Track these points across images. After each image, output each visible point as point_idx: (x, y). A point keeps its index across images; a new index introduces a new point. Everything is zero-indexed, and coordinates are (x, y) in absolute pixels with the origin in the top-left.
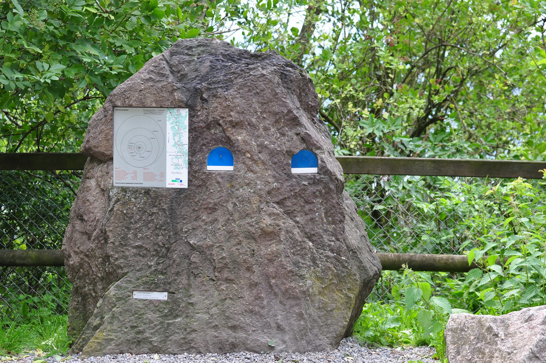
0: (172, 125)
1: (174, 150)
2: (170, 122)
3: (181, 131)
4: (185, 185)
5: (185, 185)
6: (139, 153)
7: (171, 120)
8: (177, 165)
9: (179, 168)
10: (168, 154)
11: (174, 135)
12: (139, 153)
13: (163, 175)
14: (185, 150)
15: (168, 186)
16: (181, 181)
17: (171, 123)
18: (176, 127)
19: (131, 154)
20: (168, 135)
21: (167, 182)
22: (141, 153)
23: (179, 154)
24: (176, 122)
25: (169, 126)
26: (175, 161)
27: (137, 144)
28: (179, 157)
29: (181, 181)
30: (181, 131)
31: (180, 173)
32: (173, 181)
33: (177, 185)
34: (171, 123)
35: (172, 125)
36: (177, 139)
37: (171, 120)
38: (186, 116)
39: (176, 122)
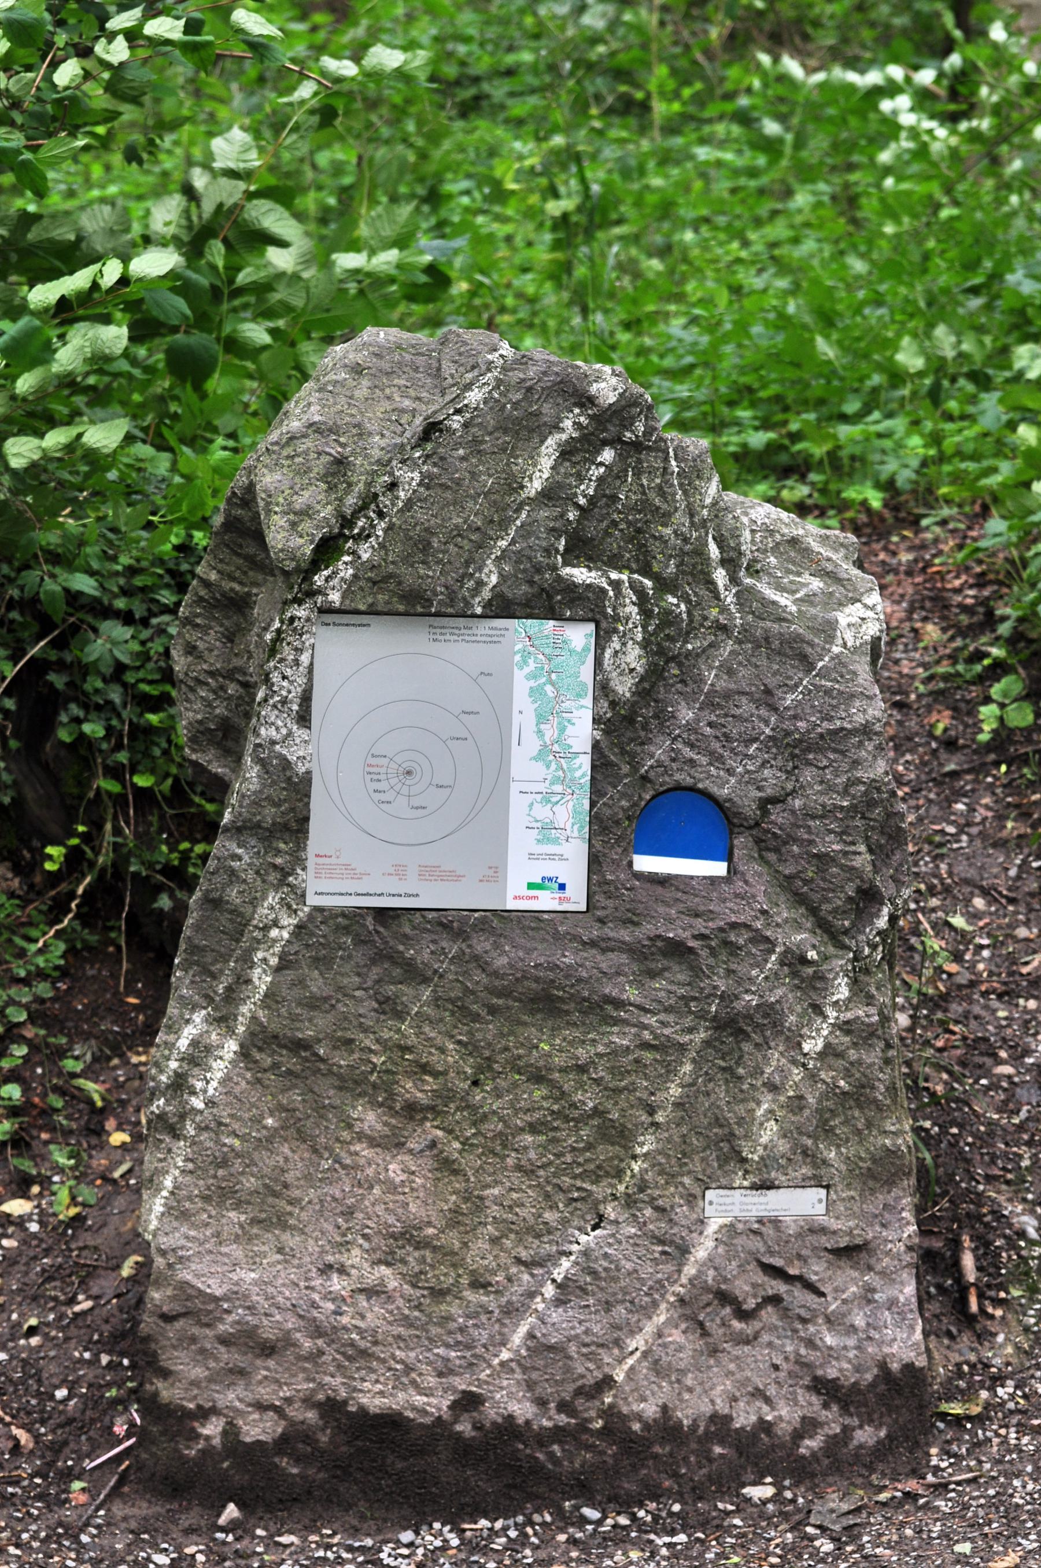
0: (532, 683)
1: (539, 770)
2: (527, 670)
3: (567, 705)
5: (577, 899)
7: (532, 665)
8: (547, 830)
9: (556, 841)
10: (514, 788)
11: (541, 719)
14: (578, 774)
16: (562, 887)
17: (528, 677)
18: (549, 688)
20: (516, 718)
21: (510, 895)
22: (414, 790)
23: (558, 788)
24: (550, 672)
25: (521, 685)
26: (543, 812)
27: (398, 759)
28: (554, 799)
29: (562, 887)
30: (567, 705)
31: (562, 858)
32: (531, 886)
33: (546, 901)
34: (530, 677)
35: (532, 683)
36: (550, 732)
37: (532, 665)
38: (586, 649)
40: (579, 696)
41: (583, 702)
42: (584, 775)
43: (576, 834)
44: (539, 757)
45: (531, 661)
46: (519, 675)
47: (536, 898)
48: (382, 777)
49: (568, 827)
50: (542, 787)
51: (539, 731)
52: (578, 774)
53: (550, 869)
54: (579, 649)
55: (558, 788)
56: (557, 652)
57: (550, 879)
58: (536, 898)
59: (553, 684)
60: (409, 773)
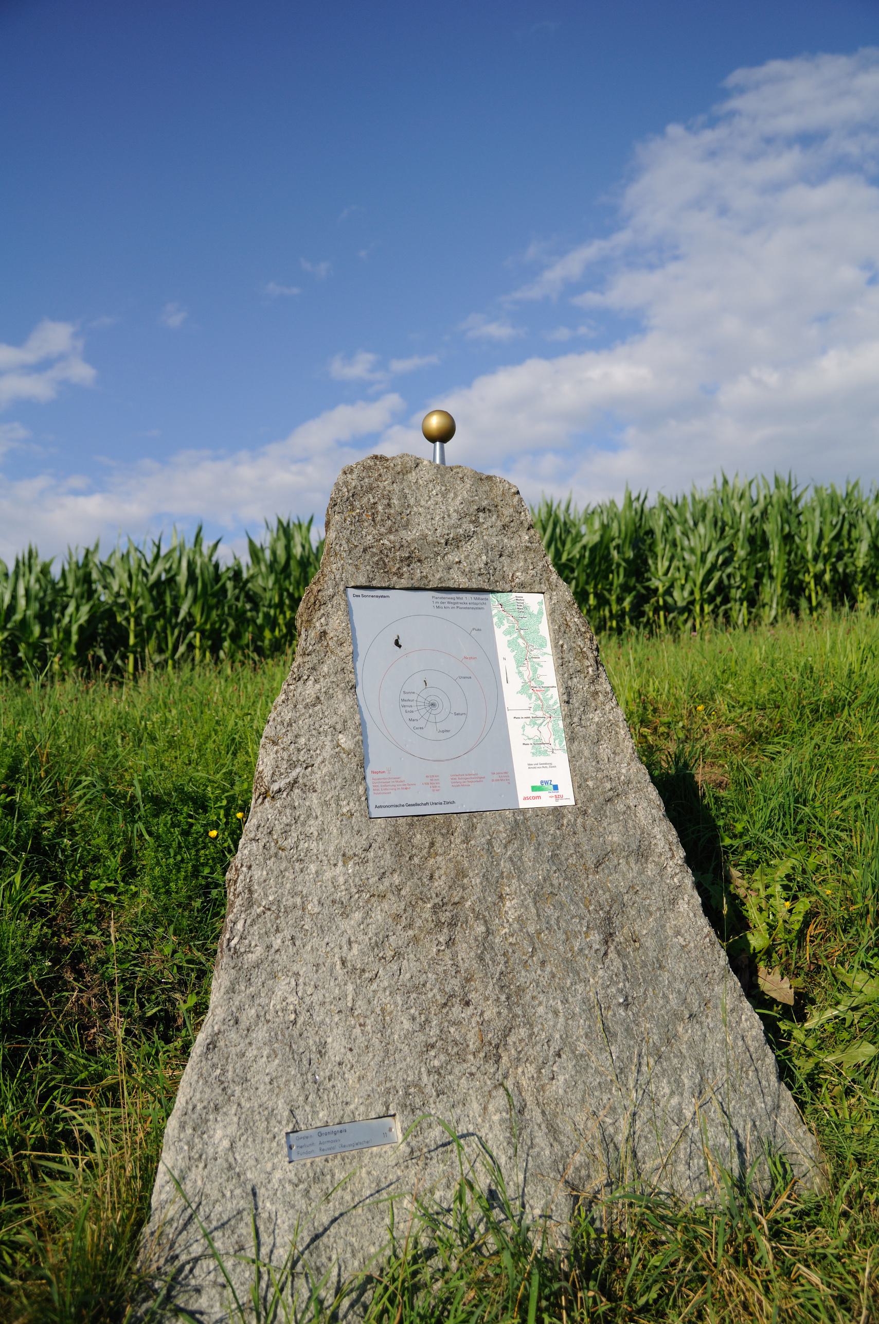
0: (508, 638)
2: (503, 628)
3: (534, 653)
4: (567, 797)
5: (567, 797)
6: (432, 718)
7: (506, 625)
8: (538, 745)
10: (510, 715)
11: (519, 664)
12: (432, 718)
13: (507, 777)
14: (551, 702)
15: (523, 805)
16: (556, 788)
17: (507, 633)
18: (520, 641)
19: (412, 724)
23: (540, 713)
24: (519, 630)
25: (502, 639)
26: (532, 732)
28: (539, 721)
30: (534, 653)
31: (551, 766)
32: (534, 789)
33: (547, 801)
34: (507, 633)
37: (506, 625)
39: (519, 630)
40: (542, 646)
41: (545, 650)
42: (555, 703)
43: (558, 747)
44: (523, 691)
45: (505, 622)
46: (499, 633)
47: (539, 797)
48: (414, 709)
49: (552, 742)
50: (528, 713)
51: (520, 672)
52: (551, 702)
53: (545, 774)
54: (536, 612)
55: (540, 713)
56: (522, 615)
57: (546, 783)
58: (539, 797)
59: (523, 639)
60: (433, 705)
